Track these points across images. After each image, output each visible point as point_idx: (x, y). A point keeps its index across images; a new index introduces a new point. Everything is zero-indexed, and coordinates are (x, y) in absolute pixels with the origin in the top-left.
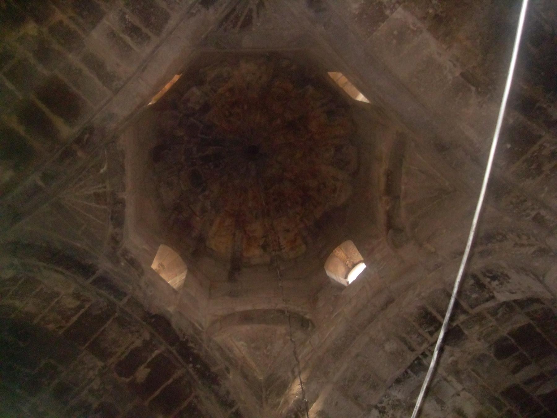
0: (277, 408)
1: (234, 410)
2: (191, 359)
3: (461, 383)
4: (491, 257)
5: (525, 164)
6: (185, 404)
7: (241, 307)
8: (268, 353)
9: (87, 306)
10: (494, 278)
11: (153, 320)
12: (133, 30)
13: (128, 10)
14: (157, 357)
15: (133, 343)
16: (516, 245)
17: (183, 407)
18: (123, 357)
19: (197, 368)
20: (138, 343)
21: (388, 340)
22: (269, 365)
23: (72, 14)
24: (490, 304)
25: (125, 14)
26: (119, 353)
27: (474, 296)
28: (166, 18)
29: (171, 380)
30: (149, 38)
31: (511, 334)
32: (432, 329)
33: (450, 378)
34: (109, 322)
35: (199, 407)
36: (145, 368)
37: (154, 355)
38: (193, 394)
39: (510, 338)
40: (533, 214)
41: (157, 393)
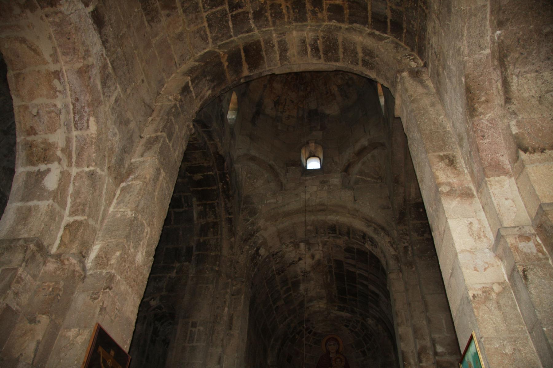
0: (247, 222)
1: (230, 217)
2: (223, 181)
3: (323, 248)
4: (377, 236)
5: (420, 225)
6: (211, 202)
7: (253, 153)
8: (253, 184)
9: (196, 142)
10: (370, 241)
11: (218, 156)
12: (316, 49)
13: (321, 40)
14: (210, 175)
15: (203, 163)
16: (389, 242)
17: (209, 202)
18: (194, 165)
19: (224, 187)
20: (205, 165)
21: (311, 225)
22: (250, 189)
23: (289, 6)
24: (362, 244)
25: (318, 39)
26: (193, 163)
27: (358, 237)
28: (337, 60)
29: (210, 188)
30: (320, 58)
31: (357, 249)
32: (331, 232)
33: (320, 244)
34: (198, 151)
35: (216, 208)
36: (201, 175)
37: (209, 173)
38: (217, 201)
39: (356, 249)
40: (406, 244)
41: (200, 189)
